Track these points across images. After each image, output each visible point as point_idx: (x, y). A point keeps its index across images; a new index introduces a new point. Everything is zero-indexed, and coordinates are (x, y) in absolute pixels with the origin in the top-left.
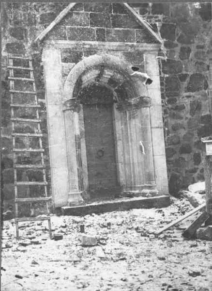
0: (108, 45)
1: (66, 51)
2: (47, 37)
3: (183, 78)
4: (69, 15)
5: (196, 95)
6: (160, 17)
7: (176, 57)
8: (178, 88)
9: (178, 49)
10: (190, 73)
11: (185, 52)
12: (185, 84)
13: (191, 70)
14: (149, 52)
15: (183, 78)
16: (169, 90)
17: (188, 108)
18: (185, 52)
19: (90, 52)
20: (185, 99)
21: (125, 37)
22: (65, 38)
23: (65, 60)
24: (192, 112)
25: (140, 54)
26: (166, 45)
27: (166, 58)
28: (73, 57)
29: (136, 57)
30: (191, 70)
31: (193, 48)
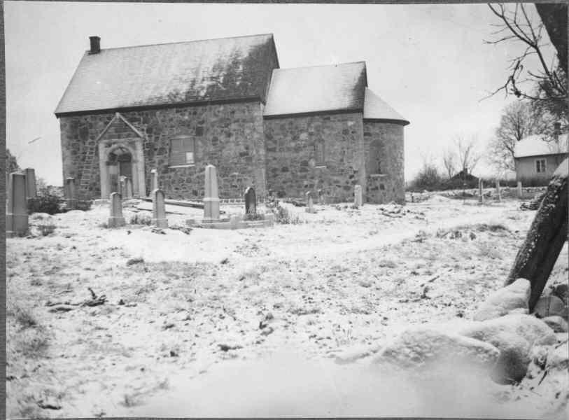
0: (122, 140)
1: (107, 143)
2: (99, 140)
3: (156, 149)
4: (107, 130)
5: (161, 157)
6: (146, 125)
7: (153, 141)
8: (153, 154)
9: (153, 138)
10: (158, 147)
11: (157, 138)
12: (156, 153)
13: (159, 146)
14: (137, 141)
15: (156, 149)
16: (149, 153)
17: (157, 162)
18: (157, 138)
19: (114, 143)
20: (156, 159)
21: (128, 136)
22: (105, 139)
23: (106, 147)
24: (159, 164)
25: (134, 142)
26: (149, 136)
27: (148, 142)
28: (109, 145)
29: (132, 144)
30: (159, 146)
31: (161, 137)
